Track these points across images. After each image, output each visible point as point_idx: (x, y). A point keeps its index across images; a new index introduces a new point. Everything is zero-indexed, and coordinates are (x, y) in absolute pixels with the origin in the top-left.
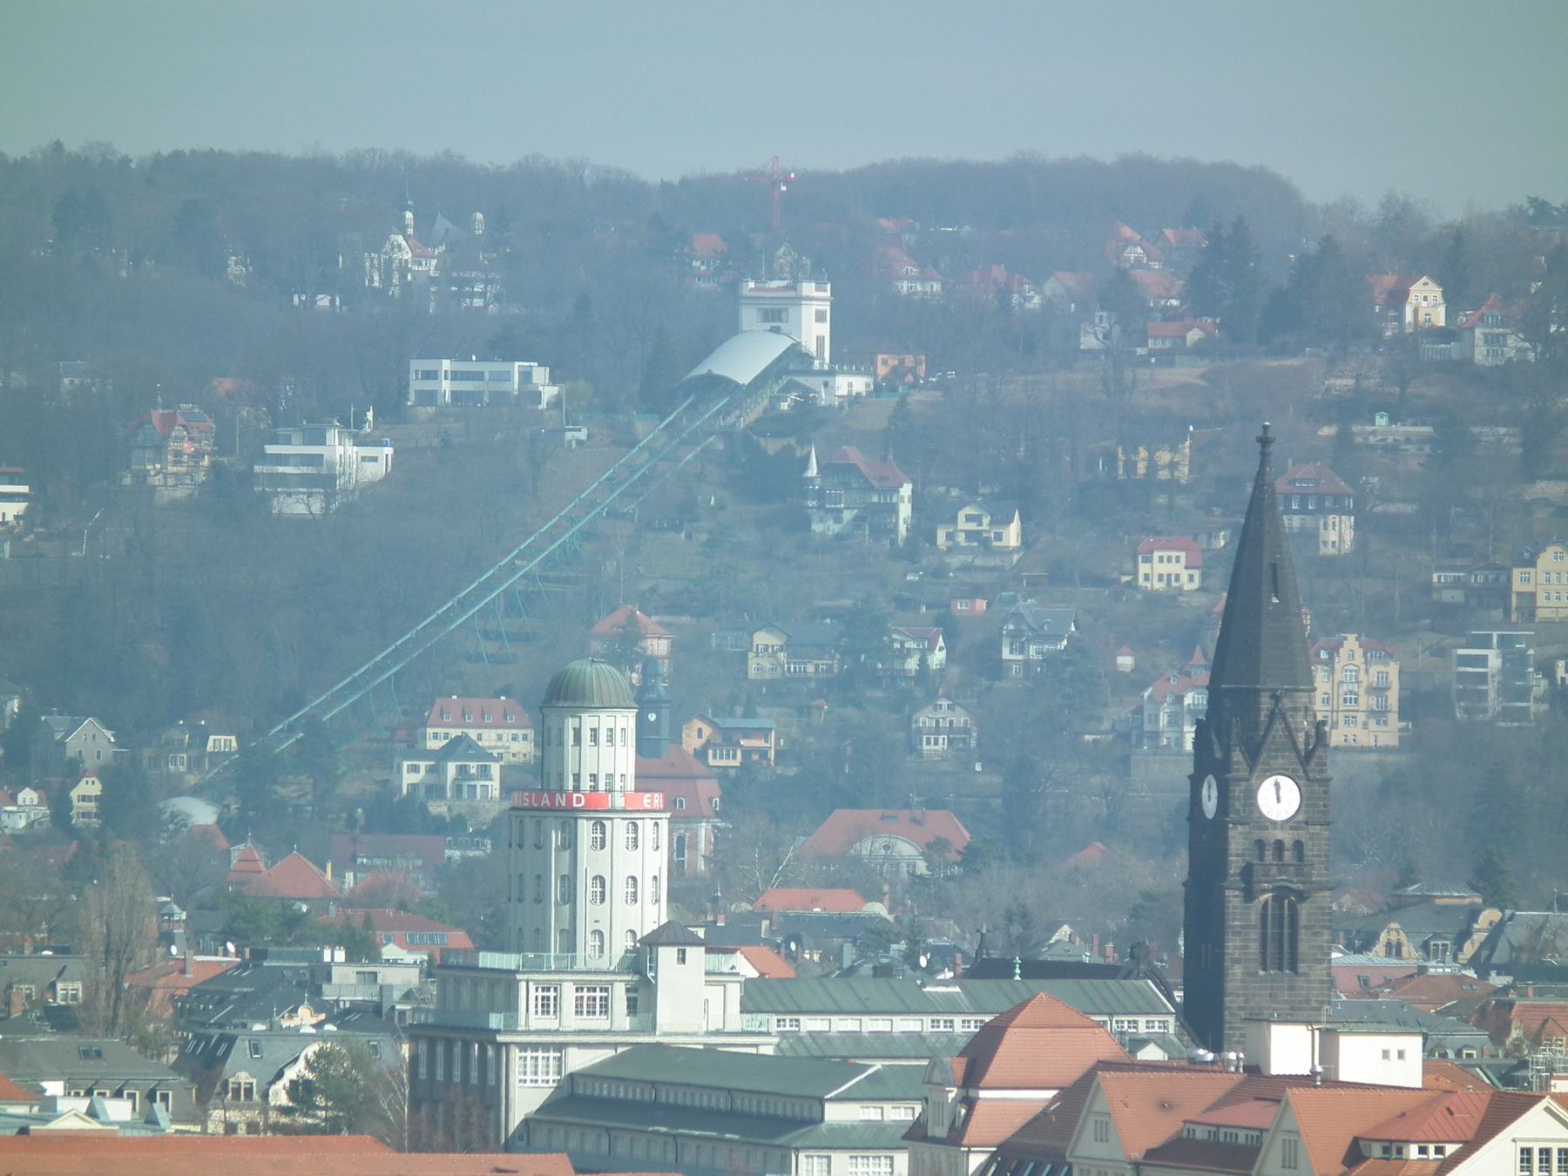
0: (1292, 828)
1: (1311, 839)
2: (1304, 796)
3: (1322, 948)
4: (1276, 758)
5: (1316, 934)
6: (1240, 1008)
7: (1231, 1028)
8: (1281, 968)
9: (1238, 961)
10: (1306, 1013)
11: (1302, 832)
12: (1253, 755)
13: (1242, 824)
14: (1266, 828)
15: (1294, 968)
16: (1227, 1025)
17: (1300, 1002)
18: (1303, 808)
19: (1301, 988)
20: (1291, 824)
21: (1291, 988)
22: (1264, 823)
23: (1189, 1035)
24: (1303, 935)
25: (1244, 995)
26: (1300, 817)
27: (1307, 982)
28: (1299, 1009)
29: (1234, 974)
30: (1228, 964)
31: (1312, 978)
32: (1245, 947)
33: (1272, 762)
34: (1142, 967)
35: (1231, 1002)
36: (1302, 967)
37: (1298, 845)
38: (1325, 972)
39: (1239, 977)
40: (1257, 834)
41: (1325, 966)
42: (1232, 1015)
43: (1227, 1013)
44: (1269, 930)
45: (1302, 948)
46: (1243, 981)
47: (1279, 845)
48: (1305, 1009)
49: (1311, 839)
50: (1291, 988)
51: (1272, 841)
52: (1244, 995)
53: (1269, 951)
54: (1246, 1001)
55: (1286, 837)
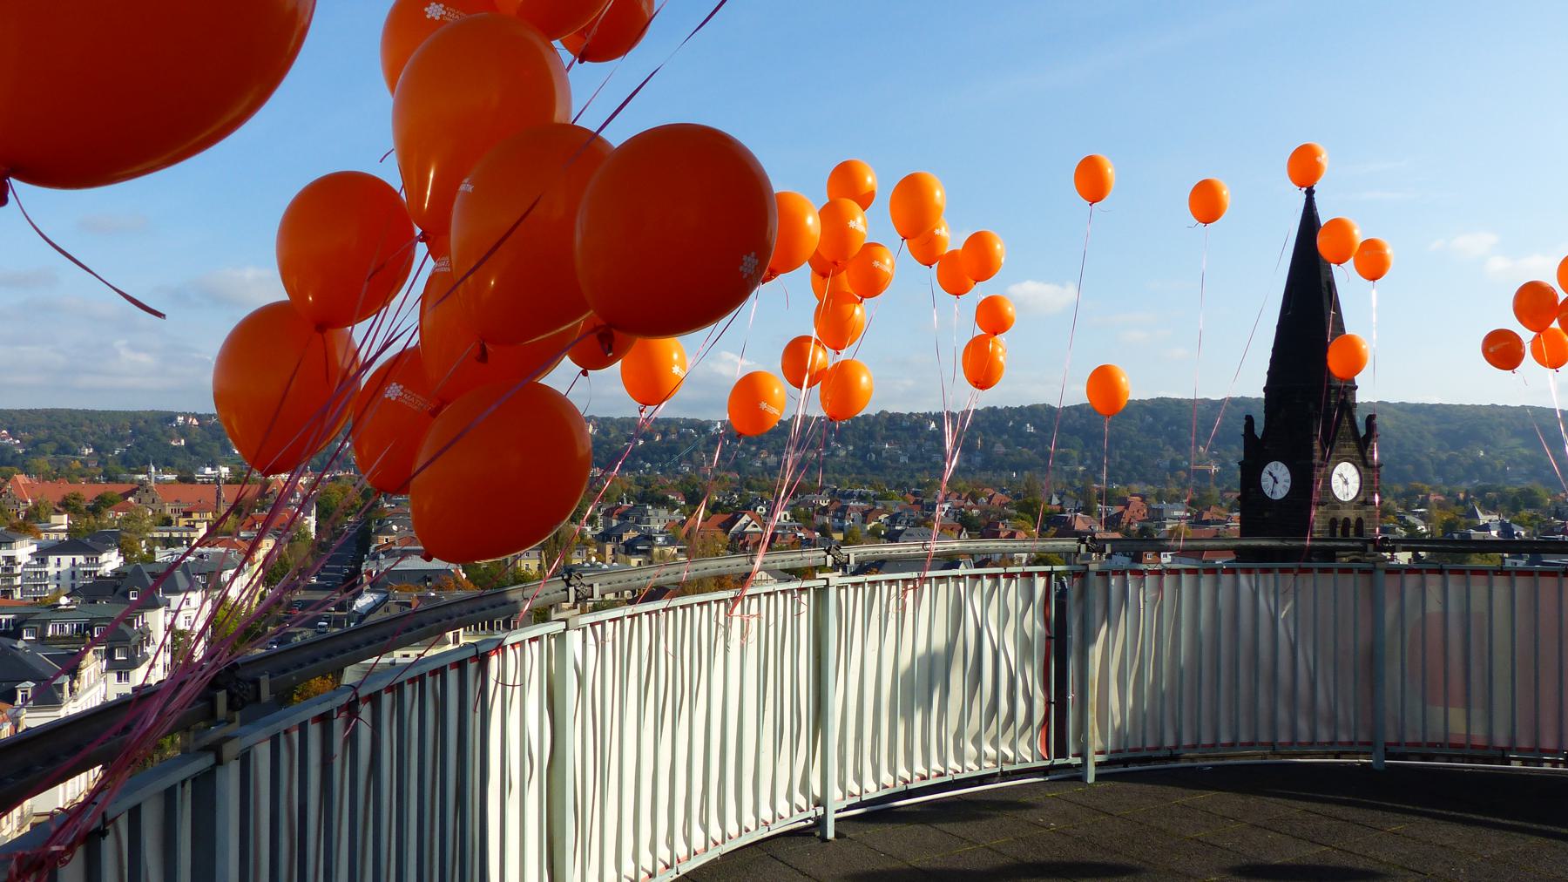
0: (1355, 508)
1: (1368, 517)
2: (1363, 479)
4: (1345, 446)
11: (1362, 511)
12: (1328, 441)
13: (1323, 505)
14: (1338, 508)
18: (1363, 490)
20: (1355, 504)
22: (1337, 504)
26: (1361, 498)
33: (1342, 449)
37: (1360, 521)
40: (1333, 513)
47: (1347, 520)
49: (1368, 517)
51: (1342, 519)
55: (1352, 515)
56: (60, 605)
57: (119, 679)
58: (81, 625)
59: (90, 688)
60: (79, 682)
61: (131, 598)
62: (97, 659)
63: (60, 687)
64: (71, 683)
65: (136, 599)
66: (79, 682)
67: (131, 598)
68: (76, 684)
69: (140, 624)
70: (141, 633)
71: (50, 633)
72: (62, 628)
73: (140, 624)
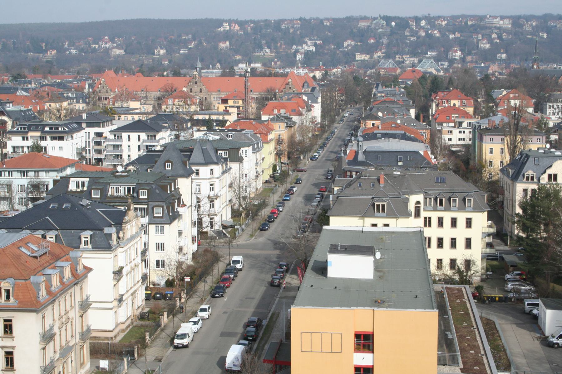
56: (118, 172)
57: (157, 231)
58: (130, 188)
59: (133, 238)
60: (124, 233)
61: (167, 169)
62: (137, 216)
63: (110, 235)
64: (118, 233)
65: (170, 169)
66: (124, 233)
67: (167, 169)
68: (121, 235)
69: (173, 189)
70: (173, 195)
71: (110, 193)
72: (118, 191)
73: (173, 189)
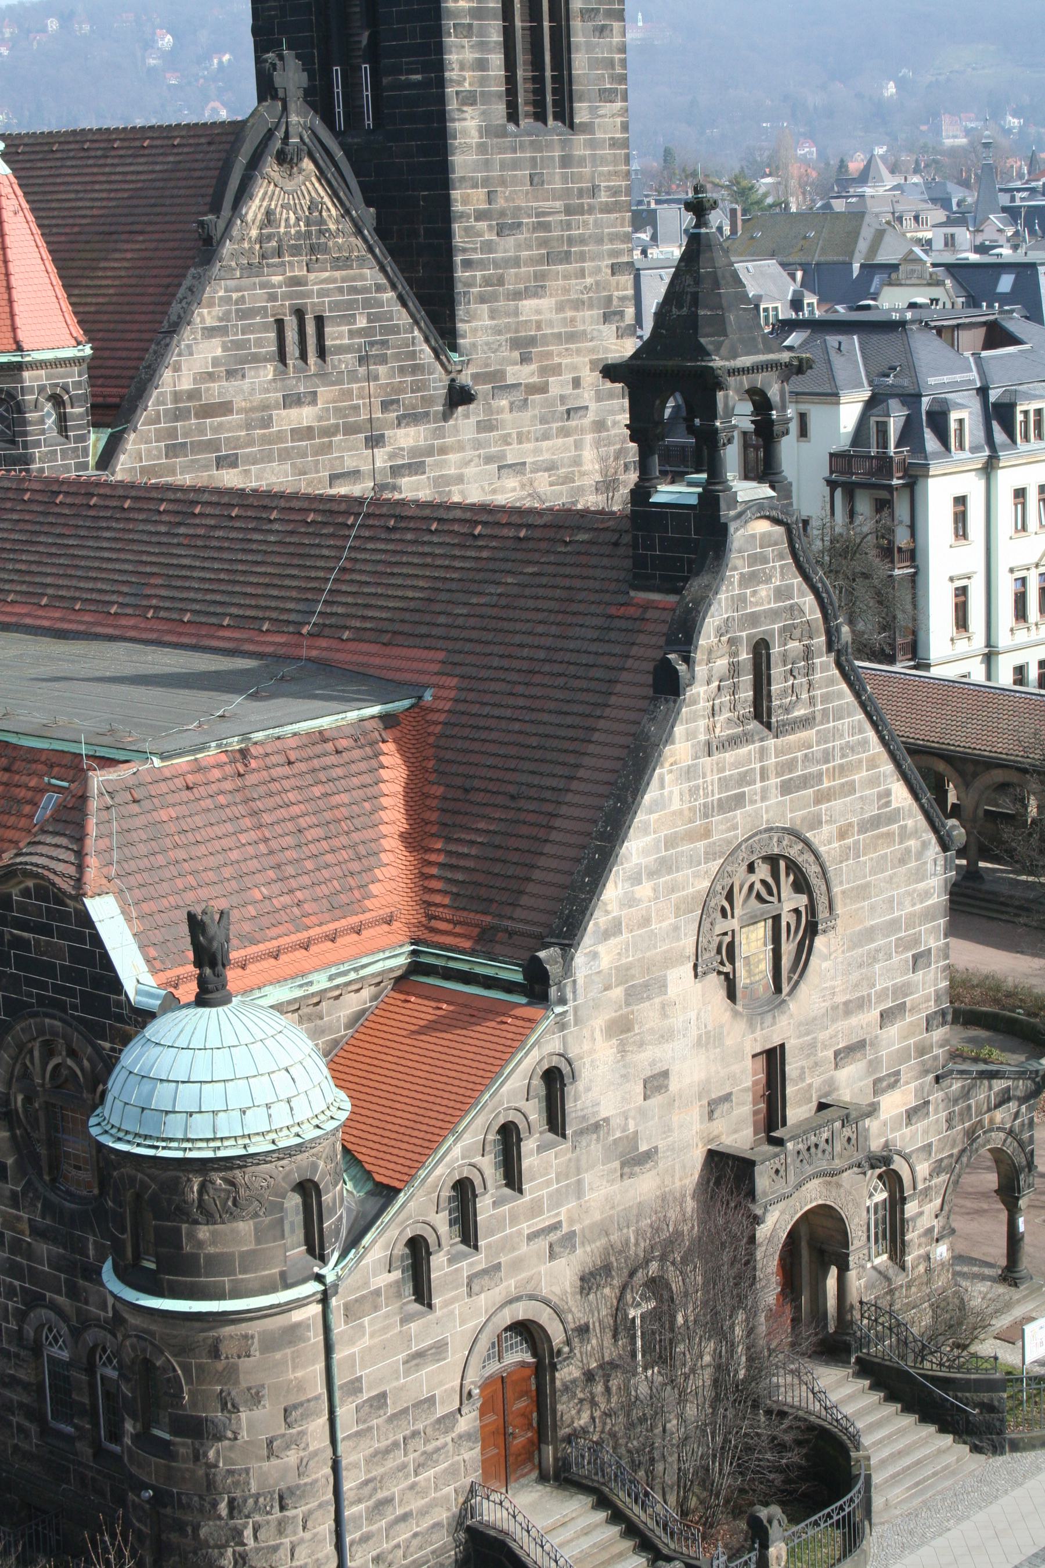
3: (611, 64)
5: (602, 30)
6: (480, 216)
7: (468, 264)
8: (540, 116)
9: (469, 99)
10: (590, 219)
15: (565, 115)
16: (458, 259)
17: (581, 193)
19: (581, 161)
21: (566, 161)
23: (394, 287)
24: (580, 33)
25: (486, 182)
27: (592, 144)
28: (580, 210)
29: (465, 132)
30: (452, 105)
31: (599, 135)
32: (481, 65)
34: (294, 119)
35: (465, 202)
36: (582, 113)
38: (619, 120)
39: (474, 139)
41: (619, 105)
42: (467, 230)
43: (456, 226)
44: (518, 24)
45: (580, 63)
46: (482, 148)
48: (591, 210)
50: (566, 161)
52: (486, 182)
53: (520, 73)
54: (490, 197)
